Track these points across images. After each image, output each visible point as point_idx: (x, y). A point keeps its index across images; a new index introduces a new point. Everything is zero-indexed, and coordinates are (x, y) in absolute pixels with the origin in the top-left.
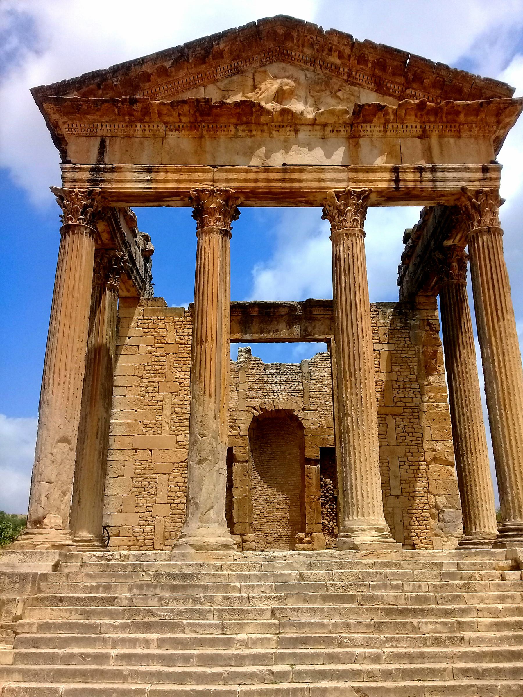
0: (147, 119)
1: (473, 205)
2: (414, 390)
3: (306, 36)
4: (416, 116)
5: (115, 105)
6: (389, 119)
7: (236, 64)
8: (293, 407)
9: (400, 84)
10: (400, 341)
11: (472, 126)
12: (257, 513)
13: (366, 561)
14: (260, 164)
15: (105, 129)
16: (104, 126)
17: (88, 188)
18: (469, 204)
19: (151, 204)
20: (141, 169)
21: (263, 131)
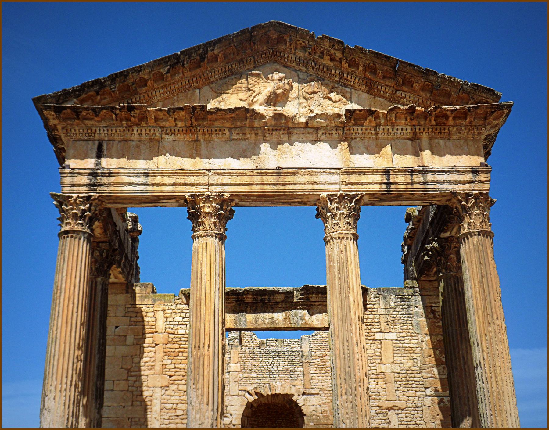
0: (144, 124)
1: (464, 207)
2: (417, 383)
4: (406, 120)
6: (380, 122)
7: (230, 67)
8: (293, 391)
10: (402, 329)
11: (461, 128)
14: (255, 167)
16: (102, 131)
17: (86, 193)
18: (459, 207)
19: (147, 205)
20: (138, 173)
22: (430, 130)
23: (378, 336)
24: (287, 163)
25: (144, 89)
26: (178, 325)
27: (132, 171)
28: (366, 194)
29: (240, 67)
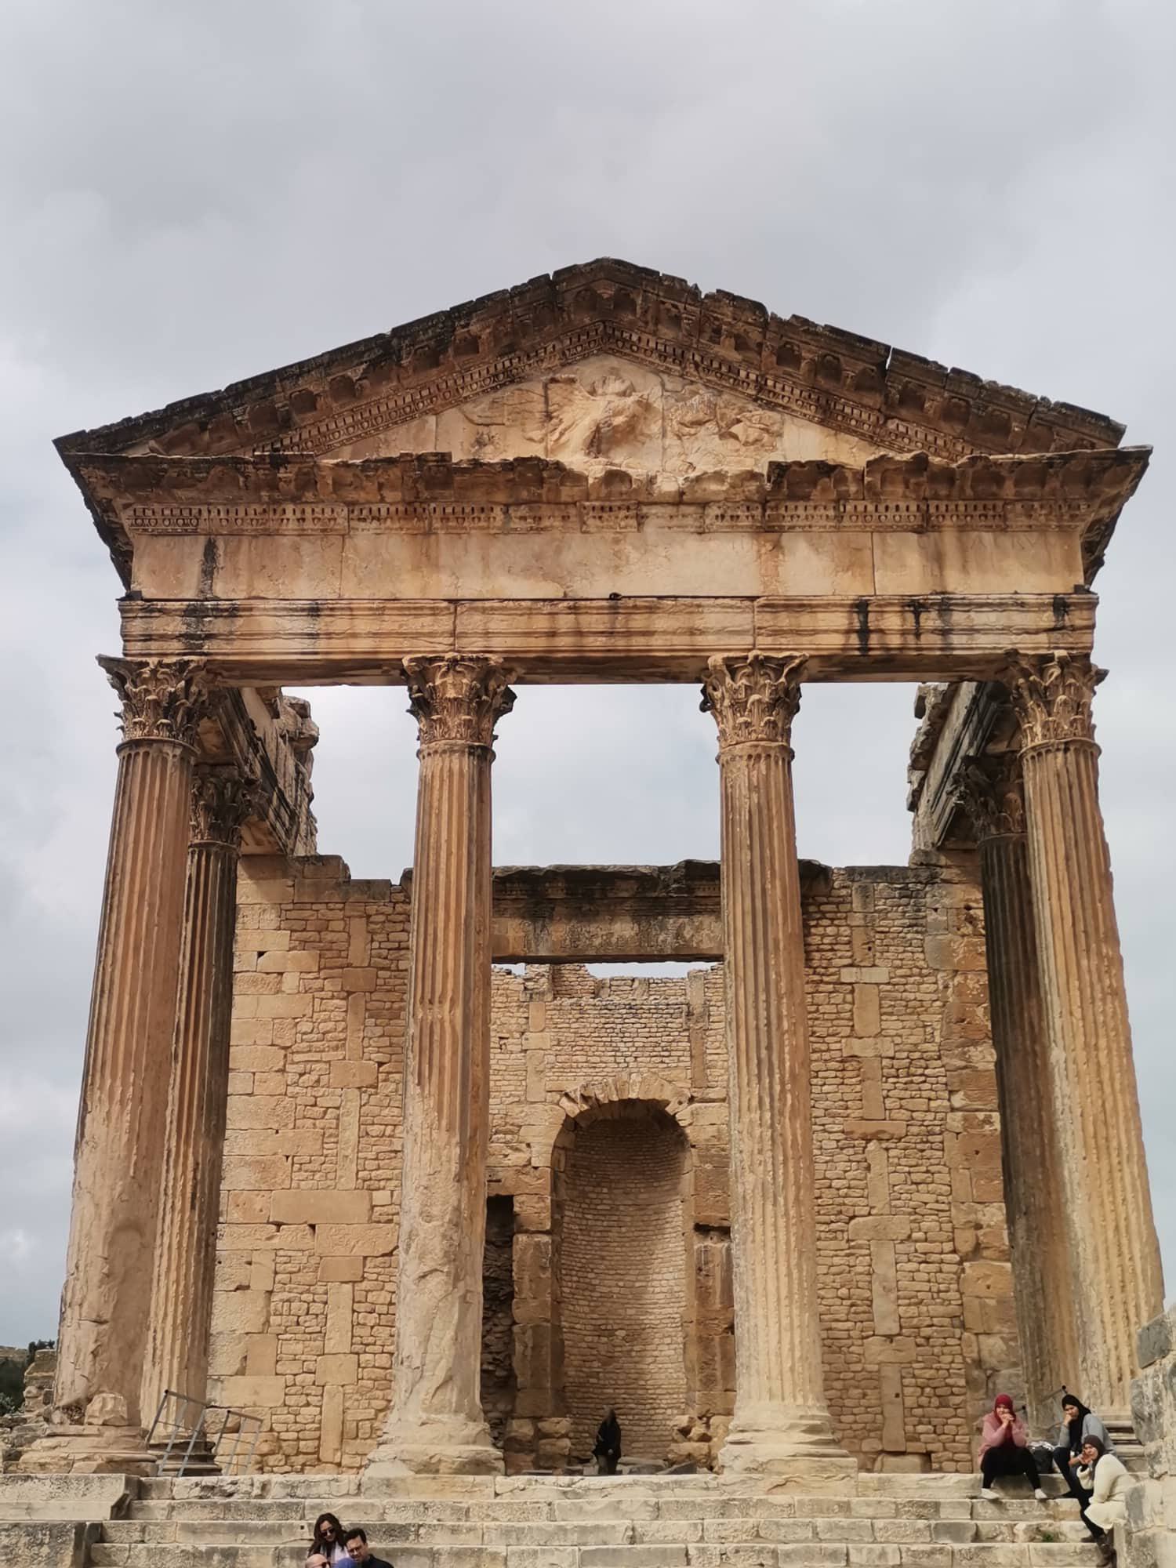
0: (309, 496)
1: (1033, 688)
2: (933, 1080)
3: (664, 303)
4: (907, 487)
5: (238, 470)
6: (848, 491)
7: (507, 364)
8: (666, 1094)
9: (872, 409)
10: (902, 960)
12: (575, 1363)
13: (779, 1498)
14: (561, 595)
15: (213, 517)
16: (214, 514)
17: (178, 654)
20: (296, 610)
21: (565, 518)
22: (962, 508)
23: (848, 975)
24: (634, 583)
25: (310, 414)
26: (399, 949)
27: (283, 604)
28: (812, 657)
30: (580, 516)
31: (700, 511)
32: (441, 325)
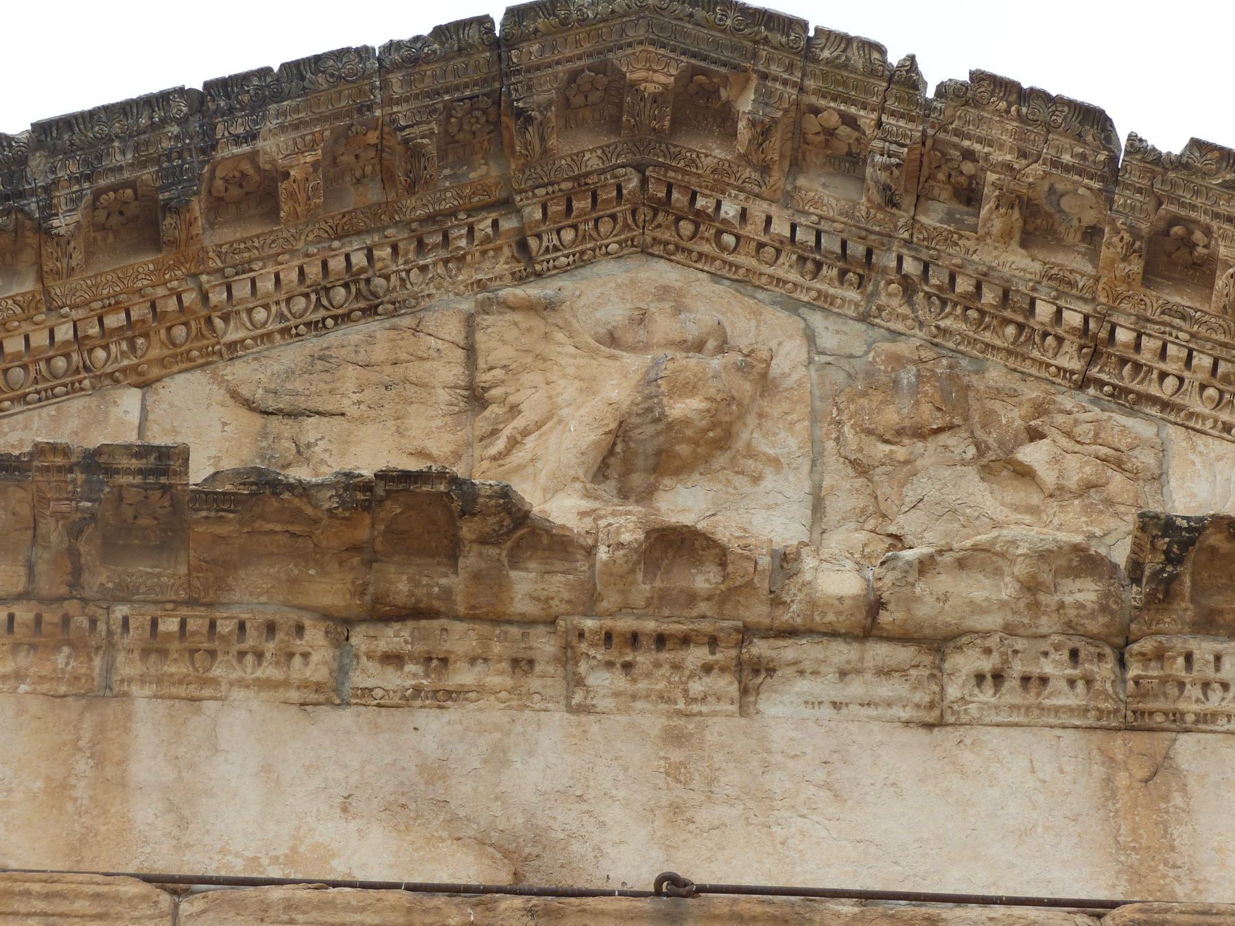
3: (816, 111)
7: (359, 259)
14: (503, 878)
21: (522, 664)
29: (424, 269)
30: (567, 656)
31: (927, 659)
32: (175, 129)
